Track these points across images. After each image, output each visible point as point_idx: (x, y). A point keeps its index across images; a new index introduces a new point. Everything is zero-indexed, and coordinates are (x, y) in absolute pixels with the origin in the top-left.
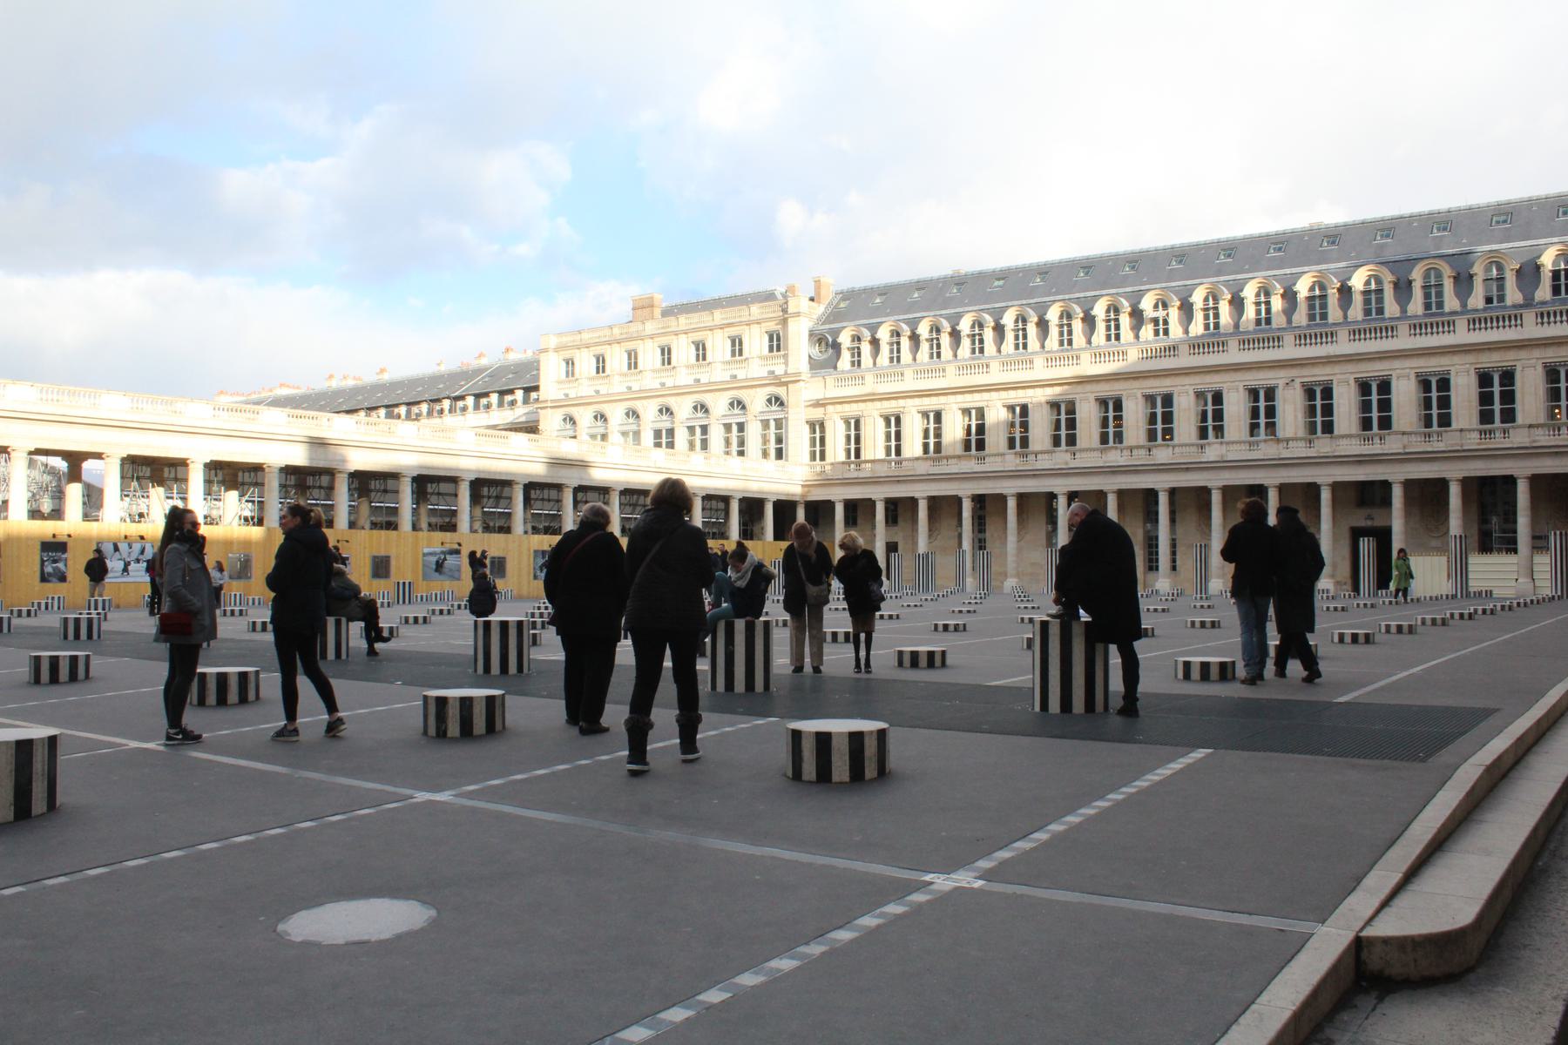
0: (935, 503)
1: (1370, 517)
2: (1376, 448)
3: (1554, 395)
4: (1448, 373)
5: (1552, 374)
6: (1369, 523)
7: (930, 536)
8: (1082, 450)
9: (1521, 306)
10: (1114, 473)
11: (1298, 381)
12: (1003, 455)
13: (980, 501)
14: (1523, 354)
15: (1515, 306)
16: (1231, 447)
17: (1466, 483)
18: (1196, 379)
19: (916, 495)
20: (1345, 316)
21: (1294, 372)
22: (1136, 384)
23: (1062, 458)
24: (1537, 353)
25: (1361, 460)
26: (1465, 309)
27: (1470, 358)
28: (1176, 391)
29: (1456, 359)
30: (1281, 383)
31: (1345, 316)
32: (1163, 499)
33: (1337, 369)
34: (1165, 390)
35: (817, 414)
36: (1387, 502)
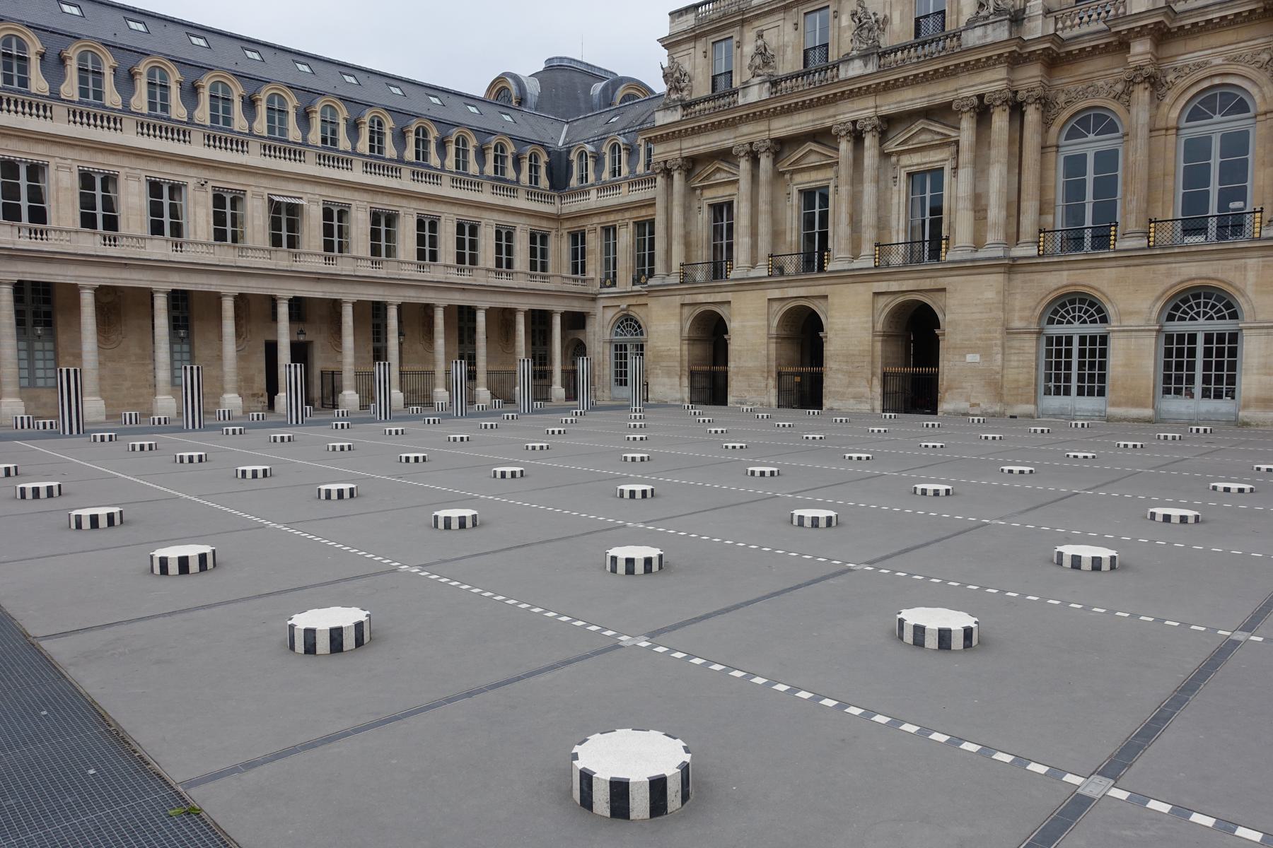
1: (302, 332)
2: (465, 278)
4: (349, 206)
6: (302, 338)
8: (122, 237)
9: (396, 161)
10: (11, 257)
11: (211, 184)
12: (143, 238)
14: (404, 202)
15: (391, 160)
16: (404, 266)
17: (447, 309)
18: (85, 156)
21: (206, 174)
24: (414, 204)
25: (319, 278)
26: (354, 152)
27: (367, 197)
28: (53, 164)
29: (356, 195)
30: (192, 183)
31: (251, 129)
34: (35, 159)
36: (274, 317)
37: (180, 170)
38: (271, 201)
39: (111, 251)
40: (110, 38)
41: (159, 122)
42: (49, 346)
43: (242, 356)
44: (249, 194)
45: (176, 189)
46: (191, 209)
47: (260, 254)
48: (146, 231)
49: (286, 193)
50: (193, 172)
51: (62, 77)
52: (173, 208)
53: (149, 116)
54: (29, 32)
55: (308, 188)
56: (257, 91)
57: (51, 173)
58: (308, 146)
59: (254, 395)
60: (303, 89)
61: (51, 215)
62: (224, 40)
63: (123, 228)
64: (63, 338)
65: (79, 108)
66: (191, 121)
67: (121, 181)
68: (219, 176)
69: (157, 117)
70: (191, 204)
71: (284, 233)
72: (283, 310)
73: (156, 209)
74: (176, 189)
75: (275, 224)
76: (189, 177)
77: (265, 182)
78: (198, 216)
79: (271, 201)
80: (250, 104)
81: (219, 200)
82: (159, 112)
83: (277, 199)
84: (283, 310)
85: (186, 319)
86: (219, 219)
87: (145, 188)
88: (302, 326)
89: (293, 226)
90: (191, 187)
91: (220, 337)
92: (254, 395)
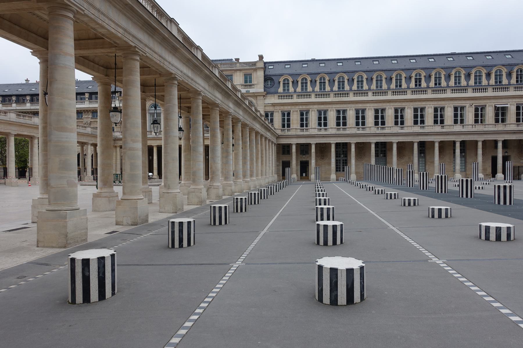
0: (442, 144)
1: (506, 152)
3: (518, 114)
5: (518, 108)
6: (506, 154)
7: (439, 157)
11: (474, 105)
13: (422, 145)
18: (436, 103)
19: (331, 142)
20: (488, 83)
22: (412, 103)
23: (417, 129)
30: (467, 105)
32: (458, 145)
33: (488, 101)
35: (271, 109)
36: (496, 147)
37: (463, 102)
38: (495, 107)
39: (444, 130)
40: (443, 66)
41: (458, 88)
42: (423, 160)
43: (484, 161)
44: (487, 106)
45: (462, 108)
46: (467, 114)
47: (491, 126)
48: (453, 123)
49: (500, 104)
50: (468, 102)
51: (430, 81)
52: (461, 115)
53: (455, 87)
54: (422, 71)
55: (510, 100)
56: (491, 70)
57: (426, 110)
58: (511, 85)
59: (487, 175)
60: (509, 65)
61: (426, 122)
62: (479, 55)
63: (446, 123)
64: (428, 157)
65: (434, 89)
66: (468, 86)
67: (446, 109)
68: (477, 102)
69: (457, 87)
70: (467, 112)
71: (500, 117)
72: (500, 145)
73: (456, 115)
74: (462, 108)
75: (497, 115)
76: (467, 104)
77: (493, 101)
78: (469, 116)
79: (495, 107)
80: (488, 75)
81: (476, 110)
82: (458, 85)
83: (498, 106)
84: (500, 145)
85: (464, 150)
86: (476, 116)
87: (453, 109)
88: (506, 150)
89: (503, 114)
90: (467, 107)
91: (476, 154)
92: (487, 175)
